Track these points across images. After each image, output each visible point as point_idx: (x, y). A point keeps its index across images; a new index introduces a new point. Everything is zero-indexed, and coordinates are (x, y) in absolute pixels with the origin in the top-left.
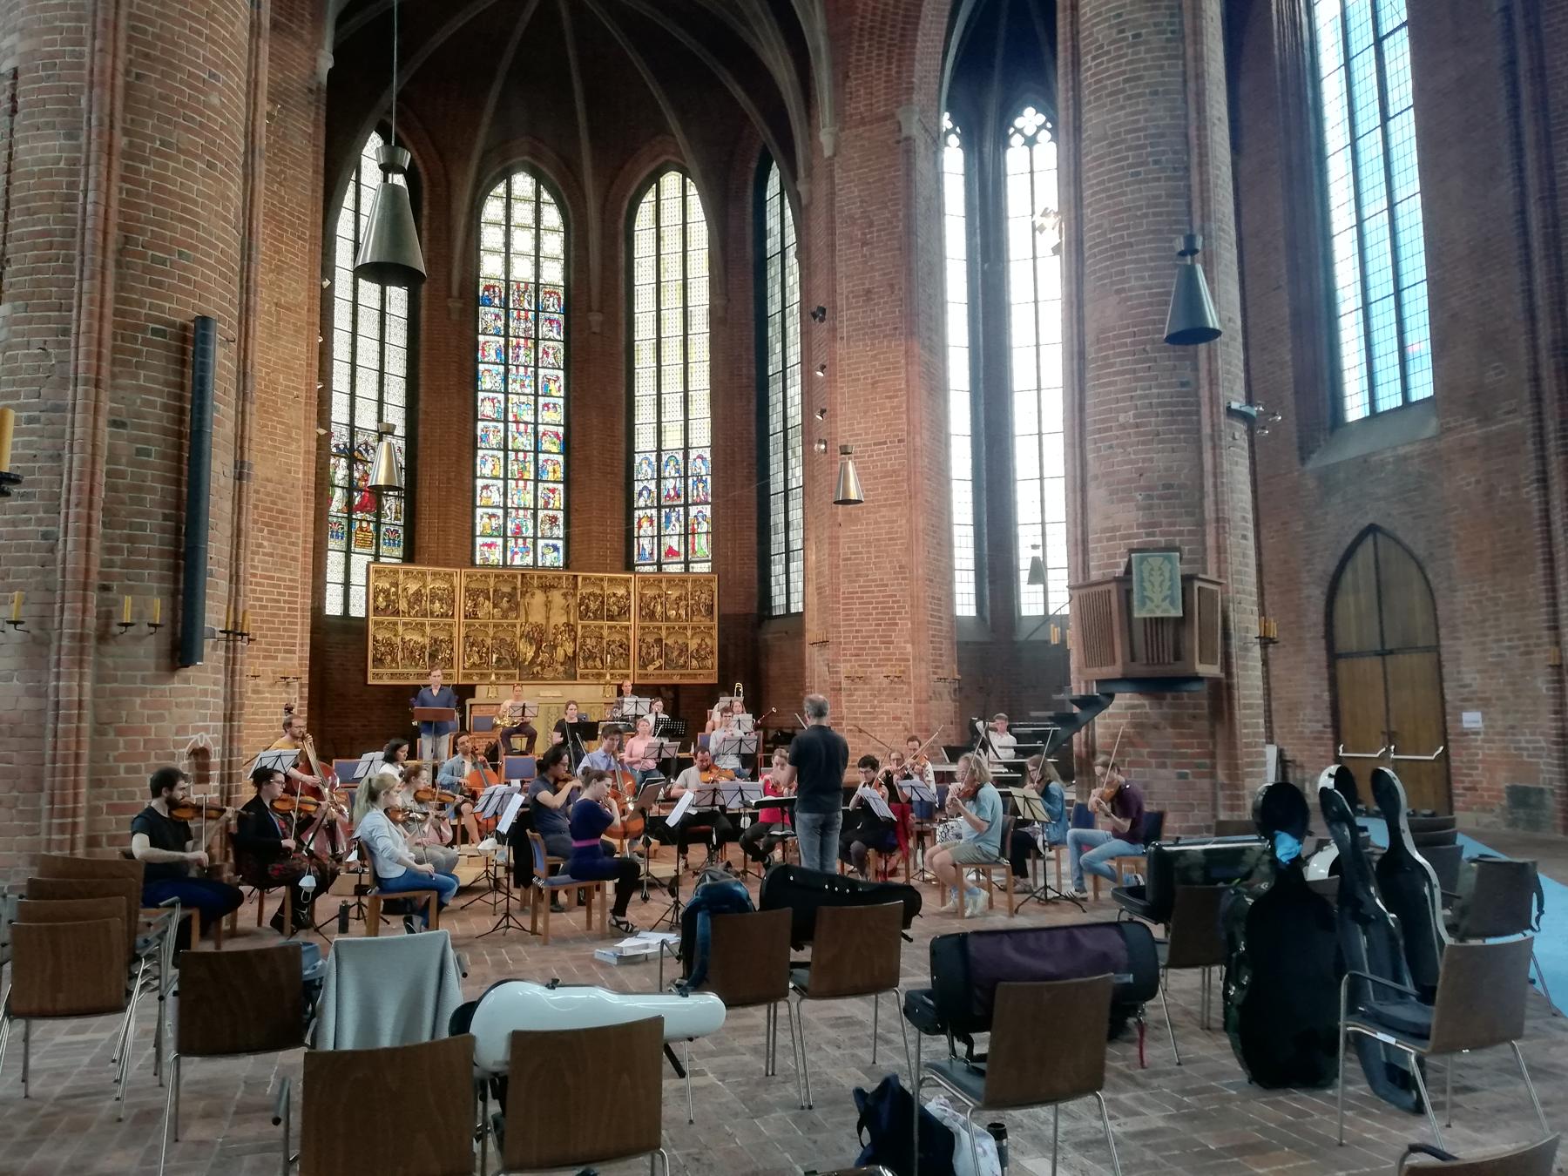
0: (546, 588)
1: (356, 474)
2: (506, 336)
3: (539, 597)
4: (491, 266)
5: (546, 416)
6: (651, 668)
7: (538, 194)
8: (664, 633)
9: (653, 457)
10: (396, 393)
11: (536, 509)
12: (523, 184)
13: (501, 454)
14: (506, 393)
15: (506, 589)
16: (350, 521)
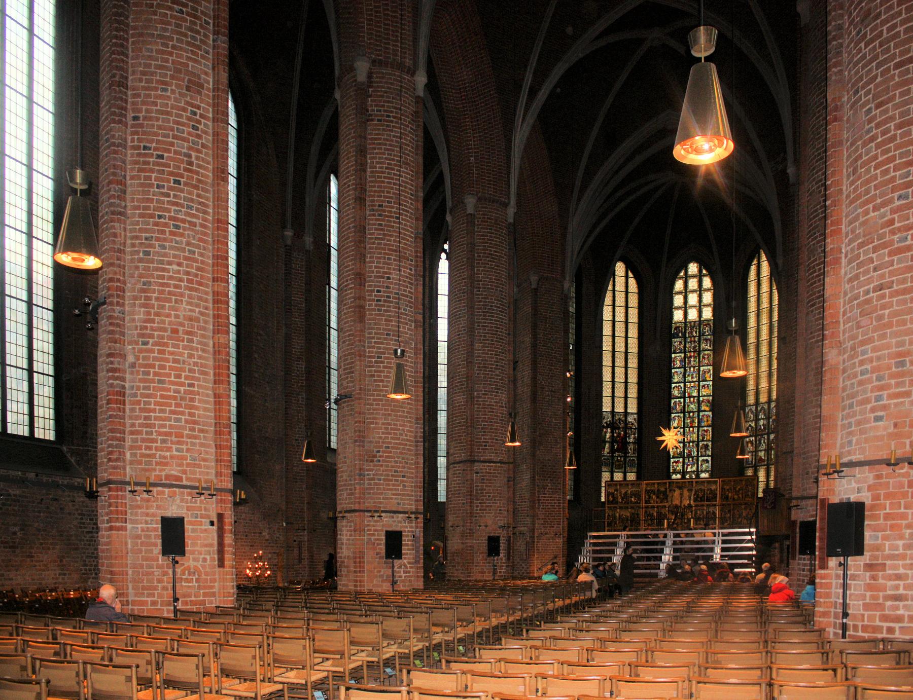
0: (680, 488)
2: (685, 353)
3: (677, 492)
4: (678, 316)
5: (704, 392)
7: (700, 271)
9: (754, 408)
10: (633, 392)
11: (698, 442)
12: (693, 268)
13: (682, 415)
14: (685, 383)
15: (662, 489)
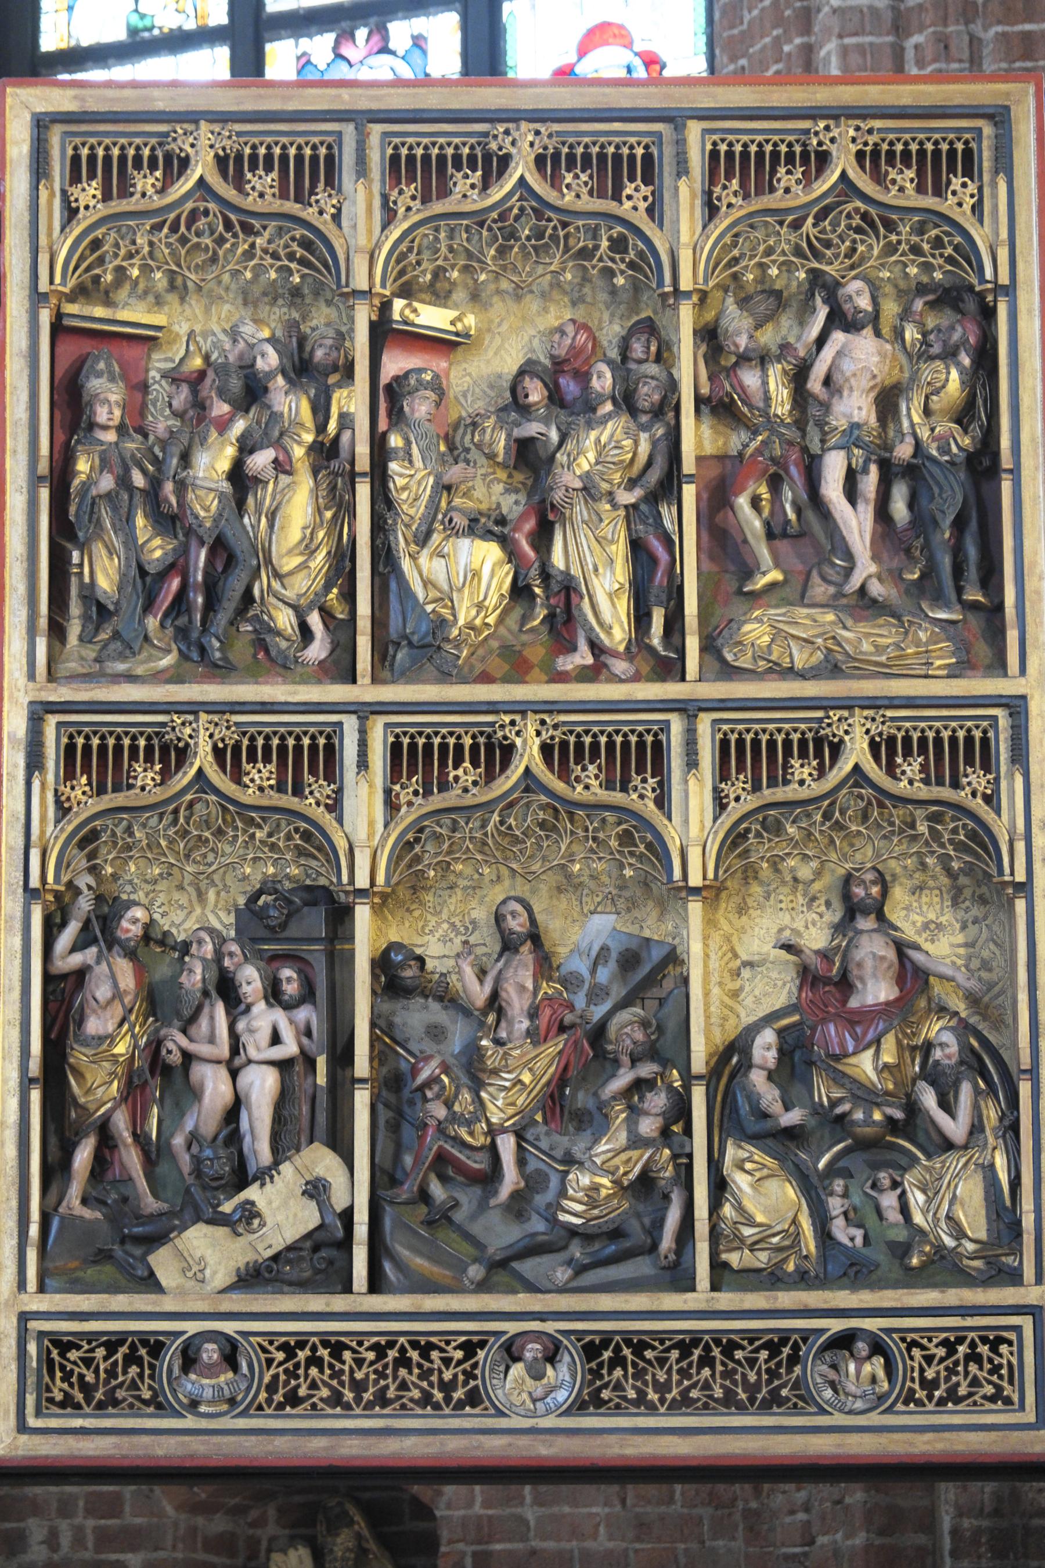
6: (202, 1259)
8: (364, 819)
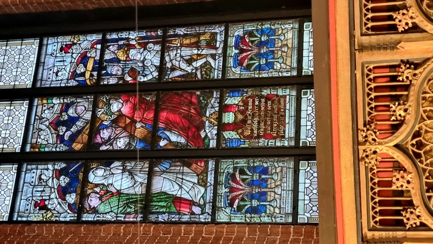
1: (121, 144)
16: (223, 153)
